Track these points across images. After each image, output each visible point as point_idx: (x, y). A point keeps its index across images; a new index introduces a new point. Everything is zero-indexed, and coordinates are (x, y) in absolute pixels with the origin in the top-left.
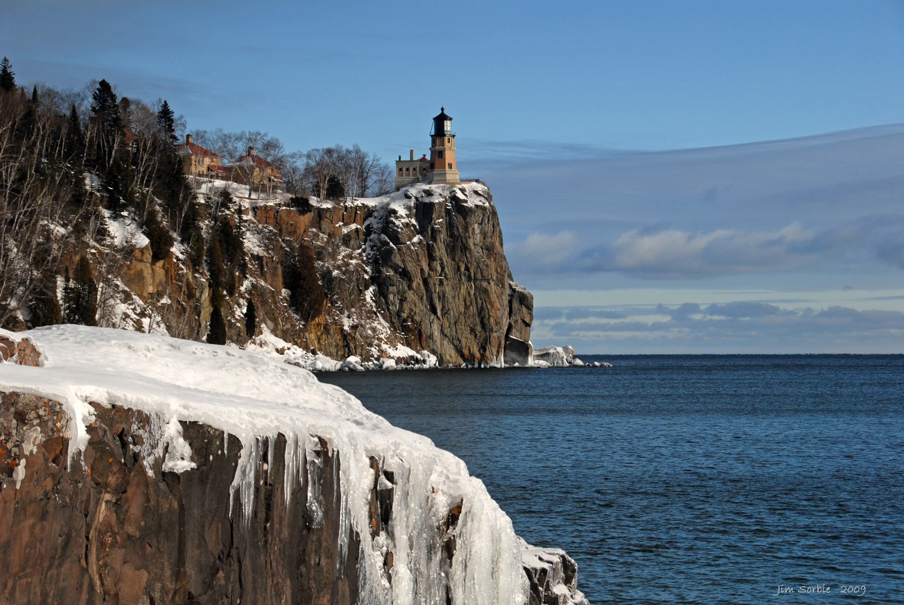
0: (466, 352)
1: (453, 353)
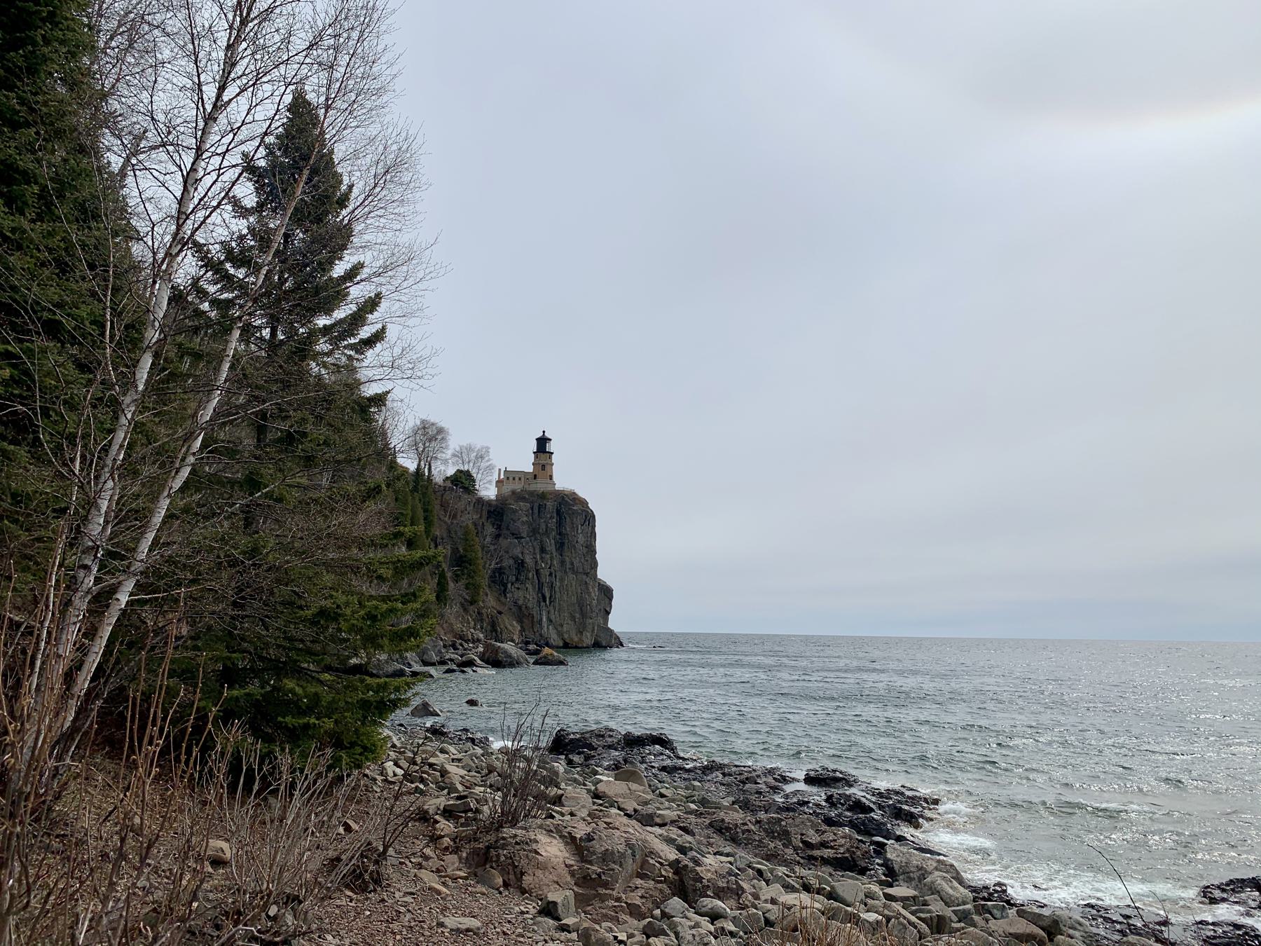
0: (566, 636)
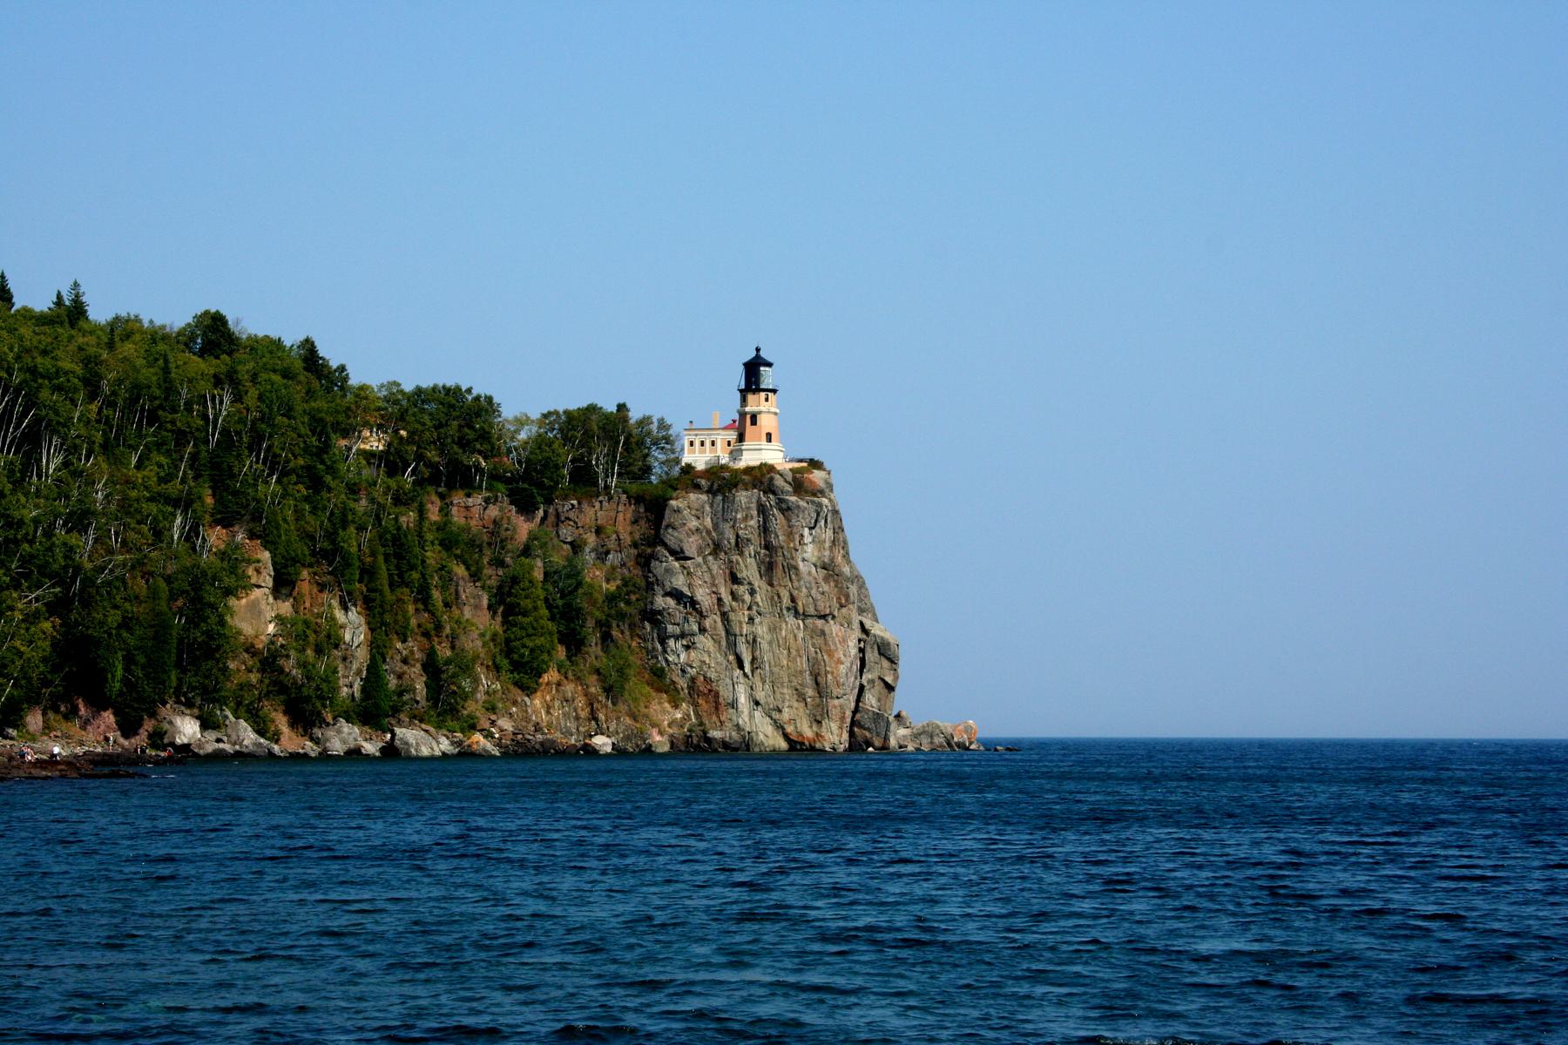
0: (790, 729)
1: (769, 729)
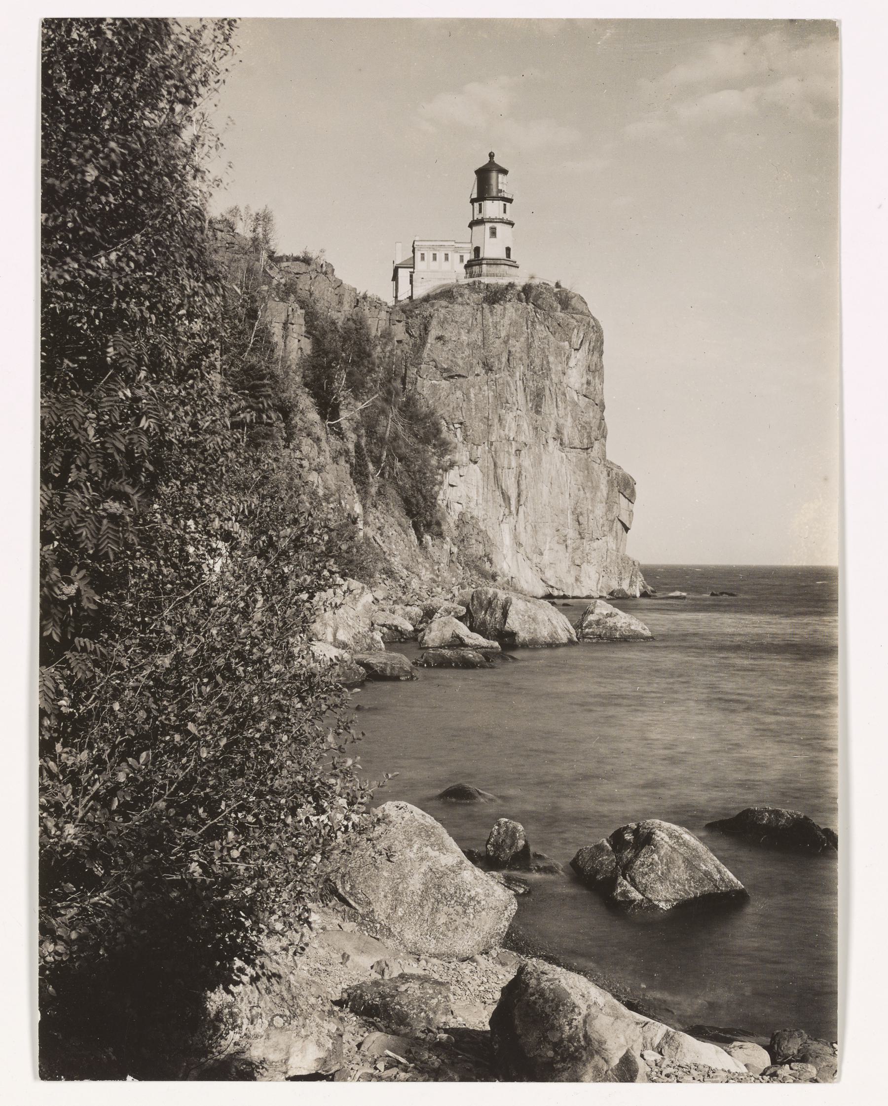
0: (549, 574)
